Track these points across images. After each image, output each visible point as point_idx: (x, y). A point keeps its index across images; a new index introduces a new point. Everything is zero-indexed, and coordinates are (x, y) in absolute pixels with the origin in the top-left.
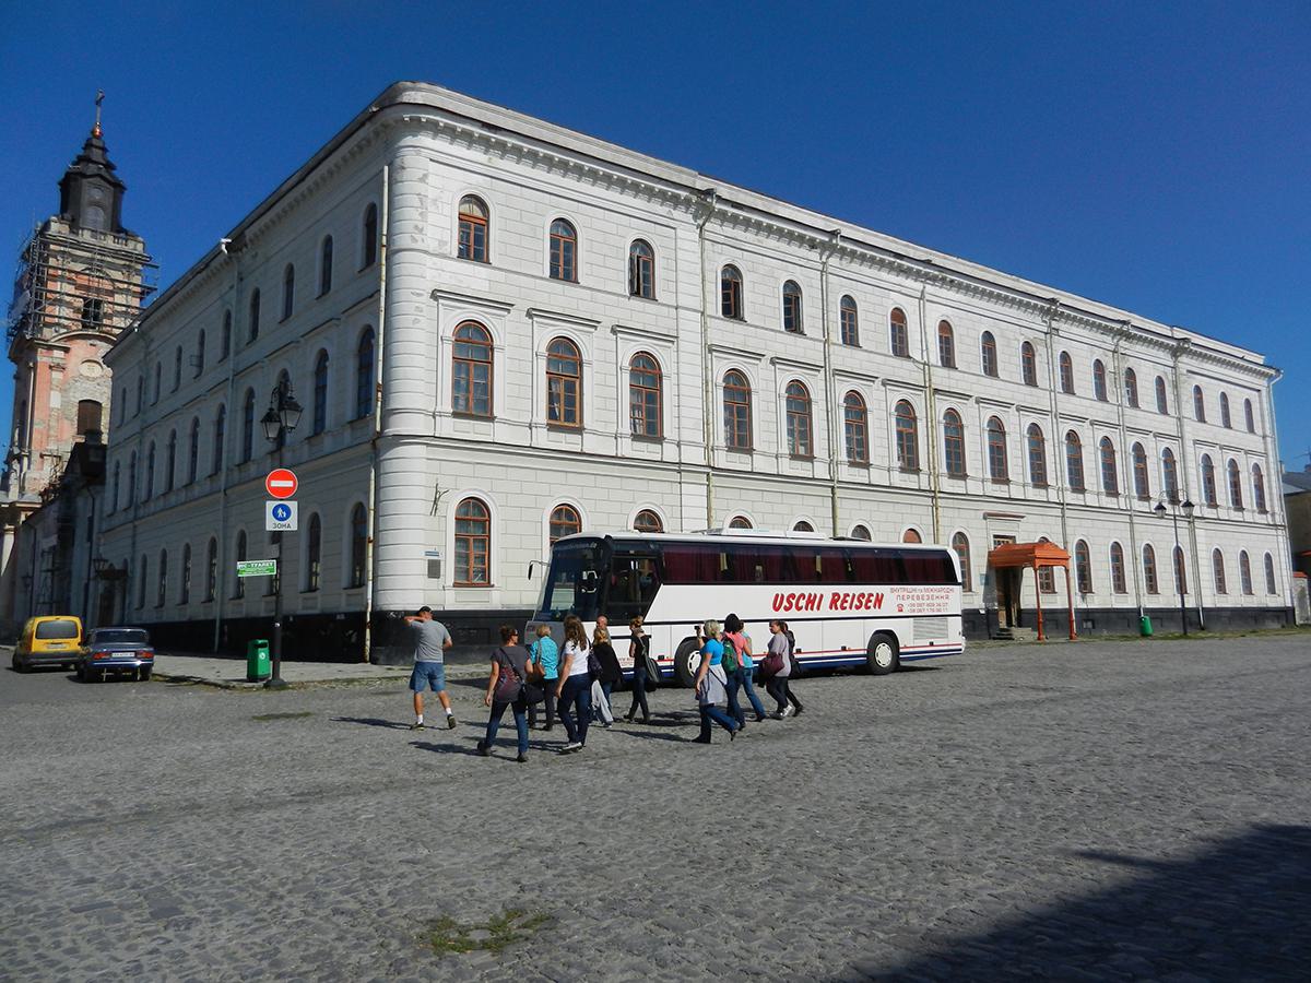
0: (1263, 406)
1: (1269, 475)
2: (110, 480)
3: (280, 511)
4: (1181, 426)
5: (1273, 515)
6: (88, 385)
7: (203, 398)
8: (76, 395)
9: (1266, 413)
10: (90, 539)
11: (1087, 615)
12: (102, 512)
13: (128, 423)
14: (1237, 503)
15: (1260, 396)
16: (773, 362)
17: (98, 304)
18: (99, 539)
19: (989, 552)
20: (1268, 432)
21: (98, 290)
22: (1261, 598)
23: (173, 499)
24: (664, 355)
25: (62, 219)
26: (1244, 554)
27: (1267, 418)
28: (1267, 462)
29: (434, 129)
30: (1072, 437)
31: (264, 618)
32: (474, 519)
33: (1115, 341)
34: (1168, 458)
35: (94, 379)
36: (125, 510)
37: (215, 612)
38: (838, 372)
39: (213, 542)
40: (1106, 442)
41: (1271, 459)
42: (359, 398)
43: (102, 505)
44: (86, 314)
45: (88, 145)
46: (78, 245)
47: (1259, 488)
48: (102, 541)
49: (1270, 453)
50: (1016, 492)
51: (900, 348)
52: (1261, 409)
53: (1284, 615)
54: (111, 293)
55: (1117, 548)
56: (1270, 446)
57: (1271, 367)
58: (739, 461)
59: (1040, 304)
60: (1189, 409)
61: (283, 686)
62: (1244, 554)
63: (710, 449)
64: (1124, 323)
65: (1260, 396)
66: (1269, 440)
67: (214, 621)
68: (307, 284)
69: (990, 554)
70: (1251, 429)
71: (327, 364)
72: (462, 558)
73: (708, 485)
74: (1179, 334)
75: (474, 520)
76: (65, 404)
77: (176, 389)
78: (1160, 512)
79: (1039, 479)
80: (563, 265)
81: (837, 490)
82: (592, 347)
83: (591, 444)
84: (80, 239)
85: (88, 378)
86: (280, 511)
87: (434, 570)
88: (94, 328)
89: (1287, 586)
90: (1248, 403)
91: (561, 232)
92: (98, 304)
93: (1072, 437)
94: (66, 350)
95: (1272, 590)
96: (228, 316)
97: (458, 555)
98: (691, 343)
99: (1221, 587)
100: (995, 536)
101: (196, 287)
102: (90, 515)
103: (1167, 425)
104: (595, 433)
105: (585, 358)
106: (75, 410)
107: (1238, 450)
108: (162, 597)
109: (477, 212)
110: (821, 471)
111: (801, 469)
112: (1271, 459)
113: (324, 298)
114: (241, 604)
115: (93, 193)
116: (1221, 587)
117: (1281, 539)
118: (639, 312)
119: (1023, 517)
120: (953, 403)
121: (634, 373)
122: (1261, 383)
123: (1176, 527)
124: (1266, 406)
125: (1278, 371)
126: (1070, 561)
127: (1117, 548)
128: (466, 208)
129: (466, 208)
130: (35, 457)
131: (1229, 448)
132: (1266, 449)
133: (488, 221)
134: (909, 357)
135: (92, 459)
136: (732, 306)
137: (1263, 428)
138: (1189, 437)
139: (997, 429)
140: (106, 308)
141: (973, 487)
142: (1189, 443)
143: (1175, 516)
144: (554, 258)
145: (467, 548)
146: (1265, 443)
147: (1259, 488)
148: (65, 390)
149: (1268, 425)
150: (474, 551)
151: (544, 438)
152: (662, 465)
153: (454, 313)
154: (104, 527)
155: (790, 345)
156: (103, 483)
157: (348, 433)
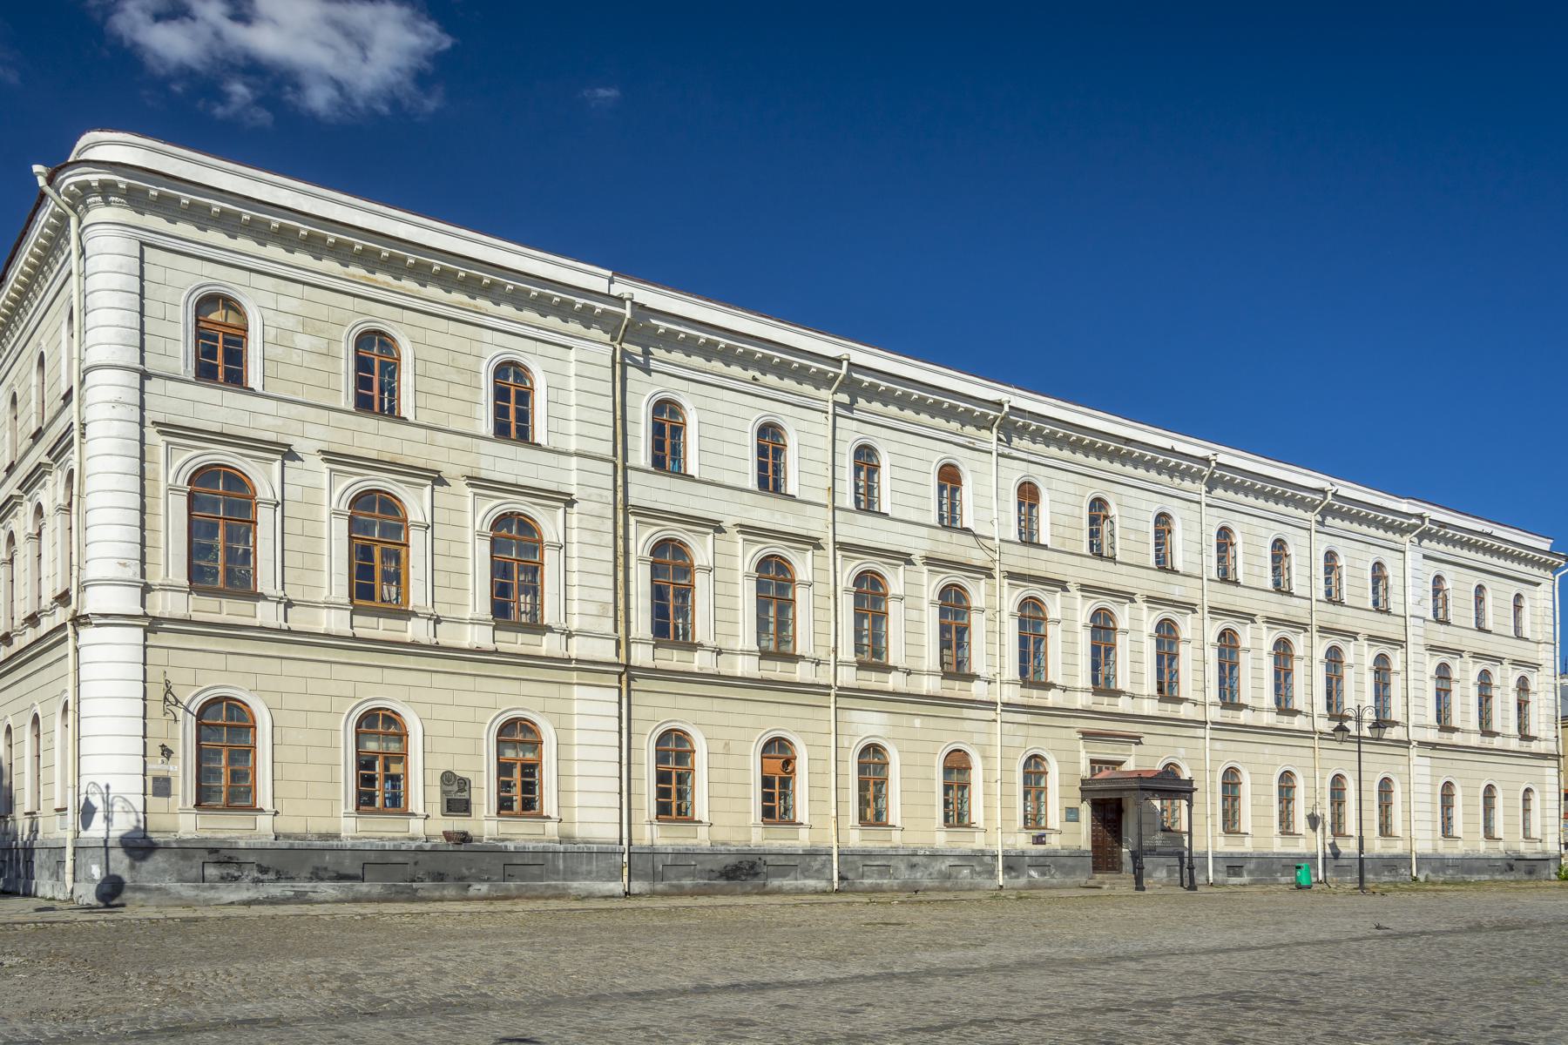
19: (1083, 781)
75: (228, 726)
78: (1339, 735)
79: (1166, 689)
100: (1093, 762)
123: (1359, 752)
143: (1359, 737)
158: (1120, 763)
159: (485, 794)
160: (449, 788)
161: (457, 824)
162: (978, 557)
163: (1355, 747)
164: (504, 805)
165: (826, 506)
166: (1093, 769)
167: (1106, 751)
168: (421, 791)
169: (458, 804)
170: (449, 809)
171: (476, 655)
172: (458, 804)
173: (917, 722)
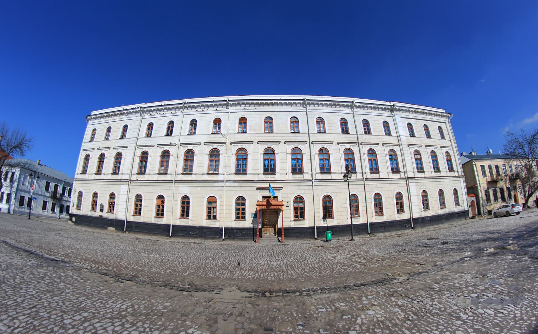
0: (447, 128)
5: (458, 172)
9: (450, 131)
14: (437, 169)
20: (452, 138)
22: (451, 207)
26: (441, 191)
27: (450, 133)
33: (352, 110)
41: (455, 149)
47: (449, 161)
49: (454, 146)
56: (453, 144)
57: (447, 113)
66: (452, 141)
74: (392, 103)
89: (465, 201)
90: (440, 128)
95: (457, 203)
112: (455, 149)
117: (462, 182)
119: (282, 188)
122: (446, 120)
124: (449, 128)
125: (450, 114)
142: (405, 148)
147: (449, 161)
149: (451, 136)
159: (106, 209)
163: (362, 183)
169: (102, 210)
172: (102, 210)
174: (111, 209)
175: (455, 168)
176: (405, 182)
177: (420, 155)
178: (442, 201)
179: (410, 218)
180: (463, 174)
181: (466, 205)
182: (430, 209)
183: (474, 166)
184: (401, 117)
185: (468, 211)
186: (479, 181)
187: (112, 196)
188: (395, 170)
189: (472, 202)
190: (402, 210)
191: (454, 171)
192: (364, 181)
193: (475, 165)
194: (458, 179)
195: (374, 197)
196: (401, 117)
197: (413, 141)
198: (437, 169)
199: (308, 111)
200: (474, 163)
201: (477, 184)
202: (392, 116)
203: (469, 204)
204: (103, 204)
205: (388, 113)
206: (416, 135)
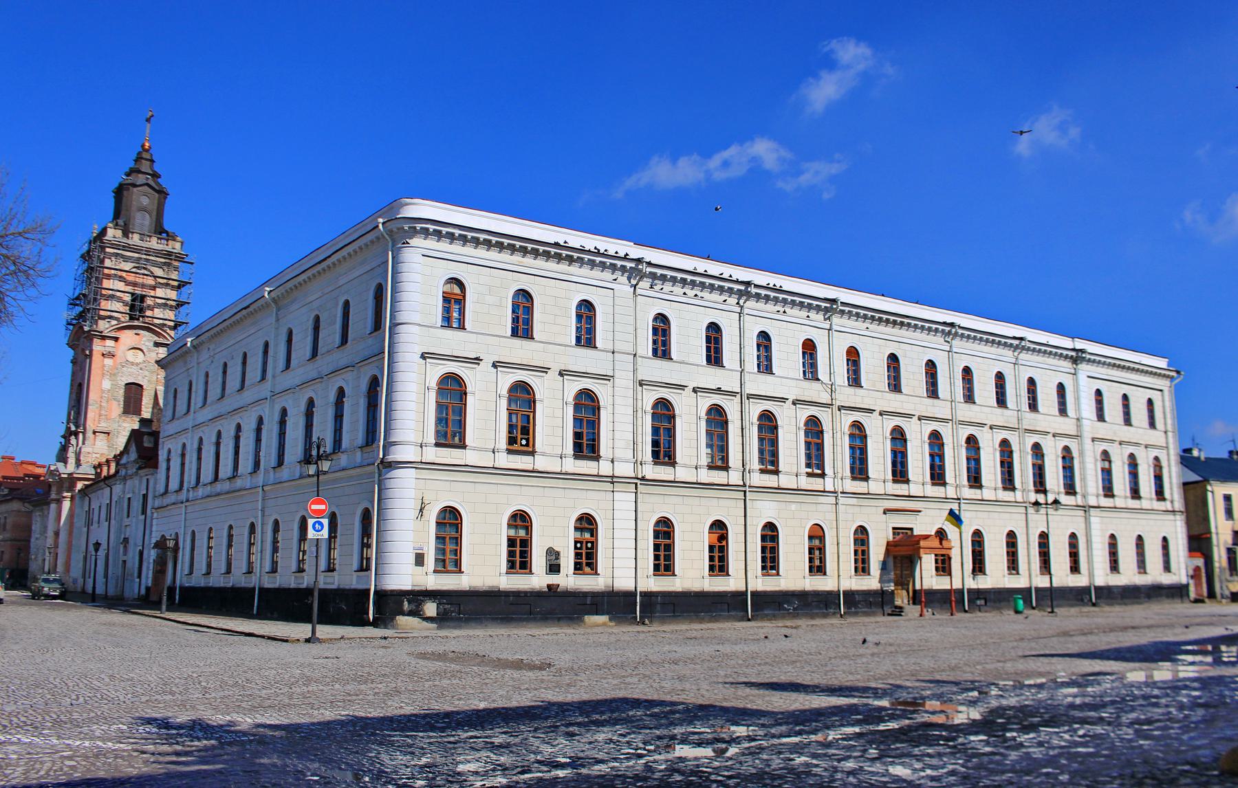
1: (1169, 466)
2: (162, 465)
3: (317, 525)
4: (1079, 426)
5: (1172, 502)
6: (134, 369)
7: (245, 409)
8: (123, 379)
10: (144, 512)
11: (976, 594)
12: (155, 491)
13: (178, 419)
14: (1135, 493)
15: (1163, 396)
16: (695, 390)
17: (143, 298)
18: (153, 513)
19: (888, 543)
21: (143, 286)
22: (1155, 575)
23: (219, 487)
24: (602, 391)
25: (116, 226)
26: (1140, 538)
28: (1168, 454)
29: (426, 232)
30: (972, 441)
31: (294, 589)
32: (450, 520)
33: (1016, 354)
34: (1067, 455)
35: (137, 364)
36: (176, 491)
37: (253, 581)
38: (750, 397)
39: (252, 526)
40: (1005, 444)
41: (1172, 452)
42: (367, 430)
43: (155, 483)
44: (132, 307)
45: (139, 159)
46: (127, 248)
47: (1158, 478)
48: (155, 515)
49: (1171, 446)
50: (914, 489)
51: (811, 370)
52: (1164, 407)
53: (1178, 592)
54: (154, 288)
55: (1011, 536)
58: (664, 473)
59: (941, 328)
60: (1089, 410)
61: (319, 641)
62: (1140, 538)
63: (638, 463)
64: (1021, 339)
65: (1163, 396)
67: (254, 589)
68: (330, 334)
69: (888, 544)
70: (1152, 424)
71: (344, 400)
72: (440, 551)
73: (636, 493)
74: (1080, 344)
76: (114, 385)
77: (223, 396)
80: (522, 327)
81: (748, 493)
82: (543, 387)
83: (540, 463)
84: (130, 242)
85: (132, 364)
86: (317, 525)
87: (420, 560)
88: (138, 319)
89: (1183, 566)
91: (521, 299)
92: (143, 298)
93: (972, 441)
94: (116, 339)
95: (1167, 568)
96: (266, 345)
97: (437, 549)
98: (624, 380)
99: (1114, 566)
100: (894, 528)
101: (241, 318)
102: (145, 492)
103: (1067, 425)
104: (543, 454)
105: (537, 397)
106: (122, 392)
107: (1137, 444)
108: (209, 565)
109: (457, 290)
110: (734, 477)
111: (718, 477)
112: (1172, 452)
113: (341, 348)
114: (275, 577)
115: (142, 199)
116: (1114, 566)
118: (584, 359)
119: (920, 511)
120: (857, 416)
121: (577, 407)
126: (953, 550)
127: (1011, 536)
128: (448, 288)
129: (448, 288)
130: (89, 434)
131: (1129, 443)
132: (1167, 443)
133: (464, 297)
134: (818, 379)
135: (146, 445)
136: (662, 349)
137: (1165, 424)
138: (1087, 435)
139: (899, 436)
140: (149, 302)
141: (874, 487)
142: (1087, 441)
144: (515, 320)
145: (444, 543)
146: (1167, 438)
147: (1158, 478)
148: (114, 375)
150: (450, 546)
151: (504, 460)
152: (598, 477)
153: (438, 368)
154: (156, 505)
155: (711, 377)
156: (156, 466)
157: (359, 454)
158: (911, 529)
159: (567, 561)
160: (551, 558)
161: (554, 579)
162: (825, 398)
164: (578, 567)
165: (747, 372)
166: (894, 533)
167: (902, 521)
168: (538, 560)
169: (554, 568)
170: (550, 571)
171: (496, 471)
172: (554, 568)
173: (793, 507)
174: (586, 558)
175: (1167, 495)
176: (1082, 513)
177: (1110, 462)
178: (1140, 558)
179: (745, 589)
180: (1183, 509)
181: (1183, 572)
182: (987, 573)
183: (1209, 495)
184: (1089, 377)
185: (1187, 586)
186: (1216, 528)
187: (586, 523)
188: (1070, 489)
189: (1197, 569)
190: (723, 566)
191: (1164, 499)
192: (1026, 507)
193: (1212, 492)
194: (1171, 517)
195: (972, 536)
196: (1089, 377)
197: (1102, 430)
198: (1135, 493)
199: (955, 350)
200: (1209, 488)
201: (1210, 533)
202: (1073, 371)
203: (1191, 572)
204: (557, 549)
205: (1067, 365)
206: (1107, 419)
